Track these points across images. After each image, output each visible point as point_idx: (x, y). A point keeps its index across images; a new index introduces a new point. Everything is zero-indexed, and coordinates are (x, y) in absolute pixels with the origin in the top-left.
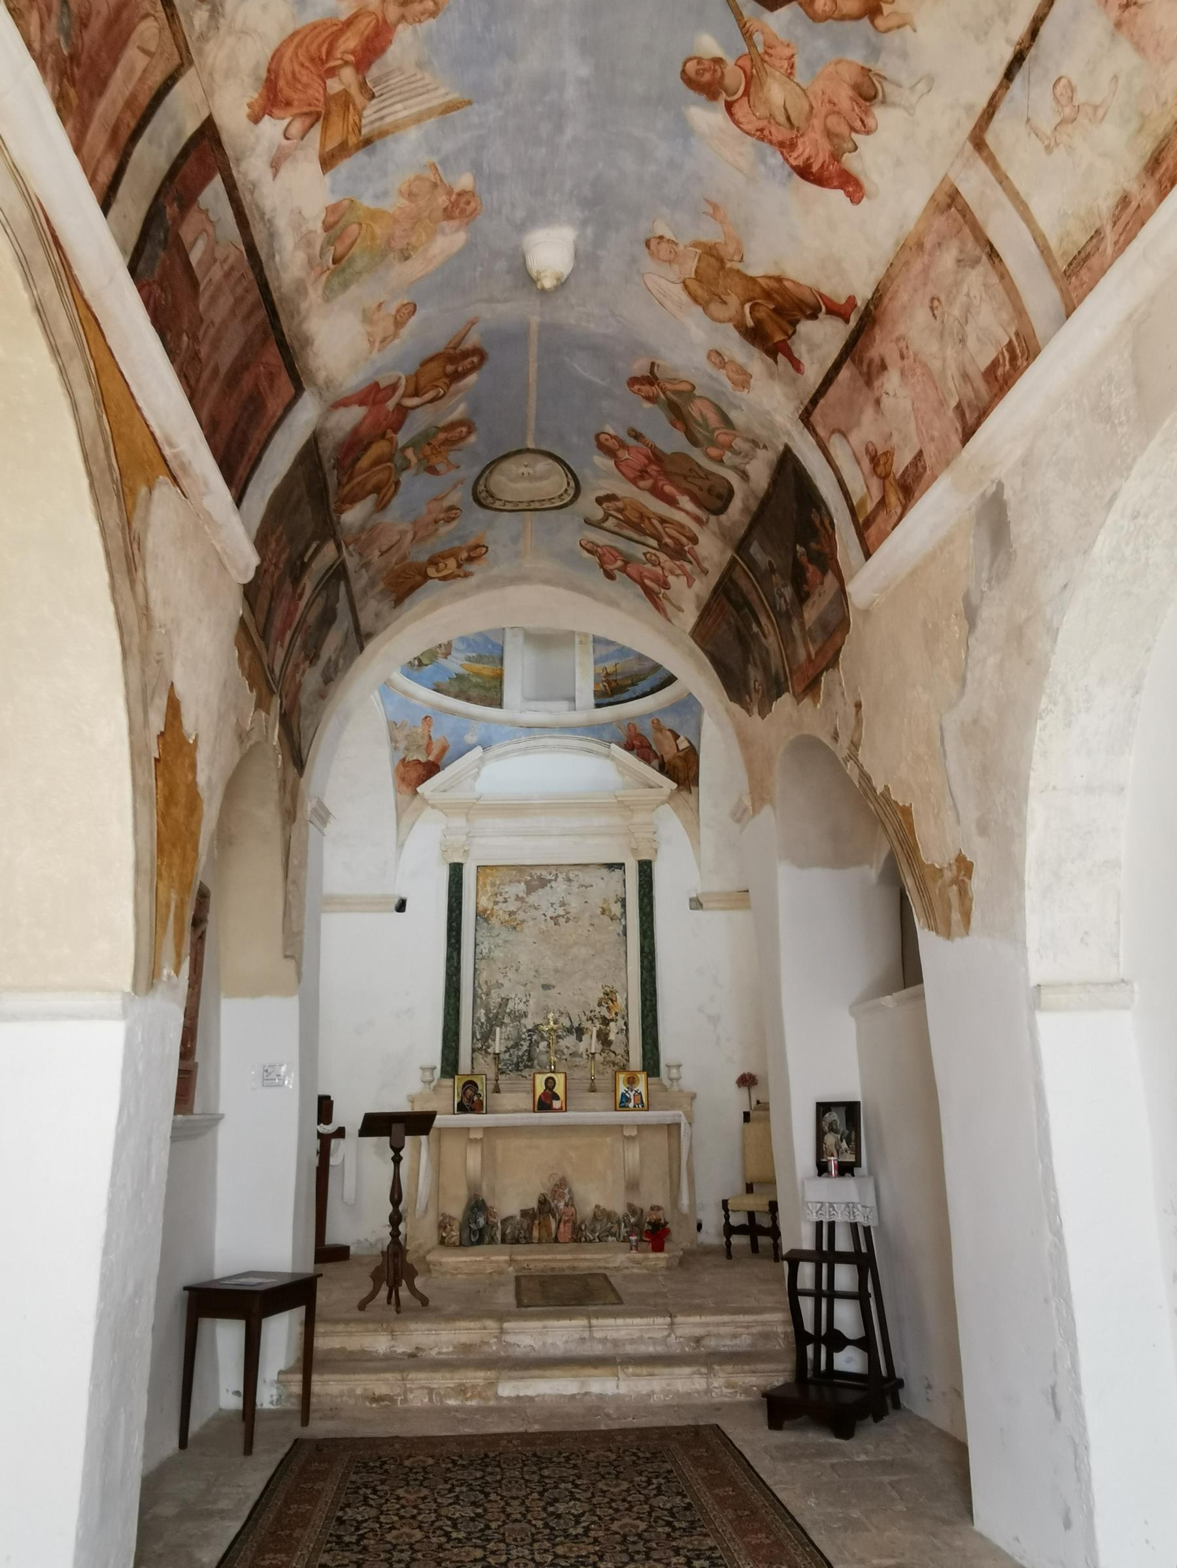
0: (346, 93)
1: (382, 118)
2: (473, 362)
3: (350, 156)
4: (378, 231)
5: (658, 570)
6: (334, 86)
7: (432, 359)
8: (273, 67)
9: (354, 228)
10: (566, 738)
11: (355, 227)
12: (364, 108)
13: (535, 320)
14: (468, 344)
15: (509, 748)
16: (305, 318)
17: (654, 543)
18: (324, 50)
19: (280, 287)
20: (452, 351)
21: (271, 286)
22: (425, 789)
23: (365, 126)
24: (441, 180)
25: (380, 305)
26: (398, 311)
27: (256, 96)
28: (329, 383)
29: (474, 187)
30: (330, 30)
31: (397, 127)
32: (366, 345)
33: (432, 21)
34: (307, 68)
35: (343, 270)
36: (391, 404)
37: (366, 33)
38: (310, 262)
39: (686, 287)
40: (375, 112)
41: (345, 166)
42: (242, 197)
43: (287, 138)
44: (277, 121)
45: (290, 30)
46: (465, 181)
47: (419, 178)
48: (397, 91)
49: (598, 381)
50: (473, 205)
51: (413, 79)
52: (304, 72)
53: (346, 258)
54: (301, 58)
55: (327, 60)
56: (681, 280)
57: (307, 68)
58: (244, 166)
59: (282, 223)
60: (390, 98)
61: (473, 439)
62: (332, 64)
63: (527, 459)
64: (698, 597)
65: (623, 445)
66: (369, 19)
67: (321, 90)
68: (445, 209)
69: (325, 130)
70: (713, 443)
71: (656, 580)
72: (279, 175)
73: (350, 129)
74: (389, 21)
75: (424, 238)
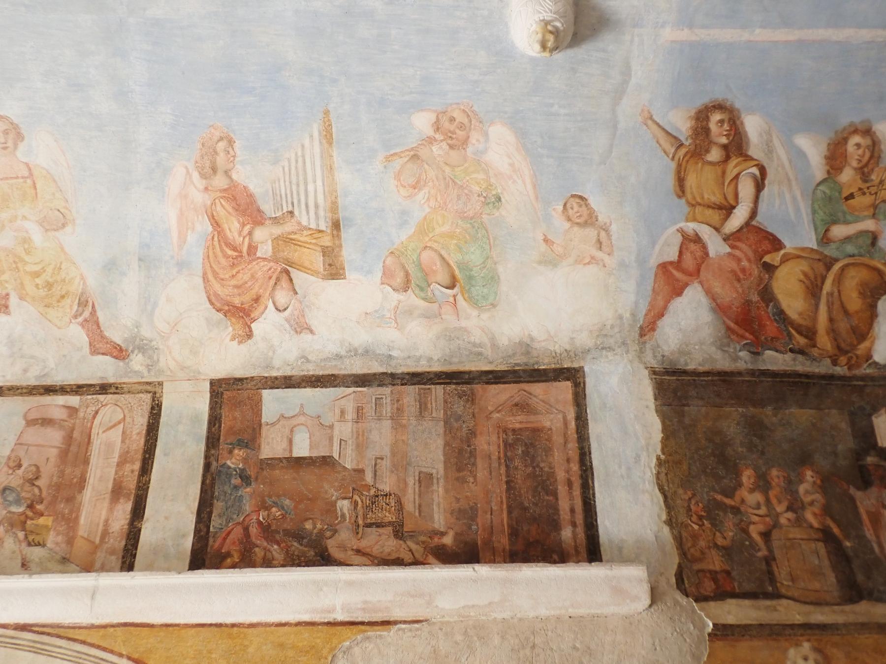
0: (276, 240)
1: (317, 206)
2: (721, 122)
3: (340, 246)
4: (446, 228)
6: (265, 250)
7: (681, 181)
8: (218, 305)
9: (426, 255)
11: (426, 255)
12: (299, 223)
13: (668, 34)
16: (493, 340)
18: (230, 252)
19: (430, 359)
20: (683, 151)
21: (419, 369)
23: (318, 225)
24: (412, 149)
25: (546, 240)
26: (569, 219)
27: (231, 329)
28: (601, 332)
29: (435, 111)
30: (216, 243)
31: (332, 193)
32: (593, 269)
33: (237, 145)
34: (238, 272)
36: (716, 247)
37: (231, 210)
38: (427, 316)
40: (308, 212)
41: (349, 253)
42: (302, 373)
43: (285, 309)
44: (264, 316)
45: (200, 281)
46: (423, 122)
47: (398, 176)
48: (294, 187)
50: (456, 114)
51: (287, 169)
52: (240, 275)
53: (457, 272)
54: (227, 276)
55: (241, 252)
57: (238, 272)
58: (277, 363)
59: (361, 338)
60: (298, 194)
62: (245, 249)
66: (219, 208)
67: (262, 264)
68: (451, 147)
69: (301, 268)
72: (313, 328)
73: (314, 241)
74: (226, 187)
75: (481, 176)
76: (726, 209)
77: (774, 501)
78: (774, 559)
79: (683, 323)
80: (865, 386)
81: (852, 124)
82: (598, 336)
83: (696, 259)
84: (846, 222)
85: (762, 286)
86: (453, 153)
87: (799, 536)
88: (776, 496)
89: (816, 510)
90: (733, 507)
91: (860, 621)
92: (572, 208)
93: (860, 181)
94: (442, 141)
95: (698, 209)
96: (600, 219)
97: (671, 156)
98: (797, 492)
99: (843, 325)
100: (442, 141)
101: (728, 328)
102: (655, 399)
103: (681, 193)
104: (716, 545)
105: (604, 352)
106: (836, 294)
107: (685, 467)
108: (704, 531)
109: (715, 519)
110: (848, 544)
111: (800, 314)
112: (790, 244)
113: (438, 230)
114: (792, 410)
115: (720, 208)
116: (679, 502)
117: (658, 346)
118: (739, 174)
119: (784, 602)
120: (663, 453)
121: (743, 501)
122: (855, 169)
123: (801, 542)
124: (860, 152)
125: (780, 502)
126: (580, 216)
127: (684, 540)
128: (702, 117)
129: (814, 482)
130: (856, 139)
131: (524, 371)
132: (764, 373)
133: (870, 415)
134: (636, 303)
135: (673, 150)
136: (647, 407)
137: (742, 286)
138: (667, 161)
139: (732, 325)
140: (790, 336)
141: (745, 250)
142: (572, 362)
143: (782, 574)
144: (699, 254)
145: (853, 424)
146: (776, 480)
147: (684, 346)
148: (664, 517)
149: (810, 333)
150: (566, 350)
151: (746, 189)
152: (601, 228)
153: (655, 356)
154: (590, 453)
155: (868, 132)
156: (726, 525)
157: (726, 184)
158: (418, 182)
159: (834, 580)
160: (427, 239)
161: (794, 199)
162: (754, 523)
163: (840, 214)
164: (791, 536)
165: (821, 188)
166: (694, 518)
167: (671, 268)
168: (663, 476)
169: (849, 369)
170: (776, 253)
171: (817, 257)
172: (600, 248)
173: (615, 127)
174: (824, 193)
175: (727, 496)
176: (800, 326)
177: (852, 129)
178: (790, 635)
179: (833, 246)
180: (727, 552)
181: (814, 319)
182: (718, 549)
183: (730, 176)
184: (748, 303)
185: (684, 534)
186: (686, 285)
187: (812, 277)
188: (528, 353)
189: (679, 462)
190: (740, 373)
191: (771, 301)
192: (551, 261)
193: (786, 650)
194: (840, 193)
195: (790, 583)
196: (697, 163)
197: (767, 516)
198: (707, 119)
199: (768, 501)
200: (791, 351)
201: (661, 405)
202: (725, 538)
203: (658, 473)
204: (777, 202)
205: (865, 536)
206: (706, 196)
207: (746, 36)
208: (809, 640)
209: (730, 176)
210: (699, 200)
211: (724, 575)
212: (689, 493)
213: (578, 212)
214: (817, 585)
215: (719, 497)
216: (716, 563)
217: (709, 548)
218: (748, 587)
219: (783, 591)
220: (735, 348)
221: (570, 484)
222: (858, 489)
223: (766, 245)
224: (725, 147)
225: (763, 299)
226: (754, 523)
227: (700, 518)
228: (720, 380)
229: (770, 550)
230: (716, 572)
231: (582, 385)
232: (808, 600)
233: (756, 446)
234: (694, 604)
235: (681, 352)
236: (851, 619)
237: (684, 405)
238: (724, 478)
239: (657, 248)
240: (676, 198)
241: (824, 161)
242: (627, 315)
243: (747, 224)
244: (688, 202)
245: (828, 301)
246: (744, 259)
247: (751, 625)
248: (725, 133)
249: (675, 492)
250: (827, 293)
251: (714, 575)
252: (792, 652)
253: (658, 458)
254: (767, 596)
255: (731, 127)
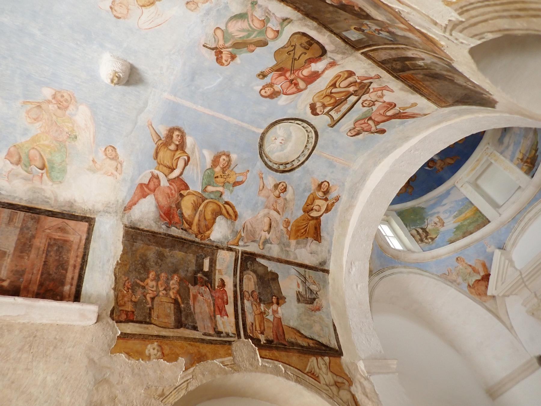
2: (178, 135)
4: (46, 143)
5: (378, 104)
7: (157, 153)
9: (32, 152)
10: (536, 206)
13: (166, 95)
14: (163, 132)
15: (514, 237)
17: (353, 98)
19: (21, 199)
20: (160, 142)
21: (14, 202)
22: (491, 291)
24: (38, 103)
25: (93, 161)
26: (106, 155)
28: (108, 205)
29: (55, 90)
35: (52, 167)
36: (164, 182)
38: (25, 179)
39: (143, 6)
46: (47, 93)
47: (28, 112)
49: (219, 80)
50: (65, 94)
53: (47, 164)
56: (140, 7)
61: (234, 157)
63: (270, 136)
64: (401, 89)
65: (271, 85)
68: (59, 108)
70: (263, 30)
71: (388, 109)
75: (70, 125)
76: (171, 169)
77: (160, 286)
78: (153, 309)
79: (143, 209)
80: (205, 247)
81: (224, 151)
82: (105, 206)
83: (155, 185)
84: (213, 186)
85: (178, 202)
86: (59, 111)
87: (165, 301)
88: (161, 284)
89: (175, 291)
90: (143, 286)
91: (179, 336)
92: (109, 151)
93: (221, 173)
94: (55, 104)
95: (161, 166)
96: (119, 158)
97: (155, 142)
98: (169, 284)
99: (203, 223)
100: (55, 104)
101: (161, 215)
102: (123, 238)
103: (156, 158)
104: (131, 301)
105: (107, 214)
106: (203, 211)
107: (128, 267)
108: (128, 294)
109: (134, 290)
110: (183, 306)
111: (189, 216)
112: (192, 189)
113: (42, 142)
114: (176, 252)
115: (169, 168)
116: (121, 281)
117: (130, 216)
118: (180, 157)
119: (152, 326)
120: (120, 260)
121: (147, 284)
122: (221, 168)
123: (165, 303)
124: (224, 162)
125: (162, 286)
126: (111, 155)
127: (119, 296)
128: (171, 131)
129: (177, 281)
130: (224, 157)
131: (67, 214)
132: (169, 235)
133: (204, 258)
134: (126, 197)
135: (157, 140)
136: (119, 240)
137: (170, 200)
138: (154, 144)
139: (162, 214)
140: (183, 223)
141: (175, 187)
142: (91, 215)
143: (154, 315)
144: (157, 183)
145: (197, 260)
146: (163, 278)
147: (141, 218)
148: (113, 286)
149: (190, 224)
150: (90, 209)
151: (181, 164)
152: (119, 163)
153: (128, 220)
154: (88, 255)
155: (228, 156)
156: (138, 293)
157: (174, 160)
158: (37, 118)
159: (174, 319)
160: (35, 144)
161: (197, 172)
162: (149, 293)
163: (212, 183)
164: (162, 300)
165: (207, 171)
166: (126, 288)
167: (144, 186)
168: (117, 270)
169: (201, 240)
170: (186, 191)
171: (200, 196)
172: (117, 171)
173: (136, 123)
174: (208, 173)
175: (142, 281)
176: (188, 220)
177: (223, 153)
178: (150, 339)
179: (207, 193)
180: (135, 303)
181: (193, 219)
182: (132, 302)
183: (176, 157)
184: (171, 207)
185: (119, 295)
186: (148, 194)
187: (196, 203)
188: (71, 207)
189: (126, 265)
190: (160, 234)
191: (179, 209)
192: (93, 170)
193: (147, 345)
194: (214, 175)
195: (157, 319)
196: (165, 148)
197: (155, 291)
198: (173, 133)
199: (157, 285)
200: (182, 229)
201: (125, 240)
202: (136, 298)
203: (116, 268)
204: (191, 172)
205: (189, 303)
206: (165, 162)
207: (194, 107)
208: (157, 342)
209: (176, 157)
210: (162, 163)
211: (131, 313)
212: (127, 278)
213: (111, 153)
214: (166, 321)
215: (138, 281)
216: (129, 307)
217: (128, 301)
218: (140, 319)
219: (153, 322)
220: (161, 223)
221: (75, 267)
222: (192, 285)
223: (183, 187)
224: (177, 145)
225: (176, 207)
226: (149, 293)
227: (128, 288)
228: (152, 235)
229: (153, 305)
230: (128, 311)
231: (93, 225)
232: (161, 326)
233: (158, 263)
234: (115, 324)
235: (139, 221)
236: (176, 334)
237: (135, 242)
238: (142, 274)
239: (140, 177)
240: (153, 159)
241: (211, 162)
242: (121, 201)
243: (178, 177)
244: (158, 163)
245: (200, 213)
246: (173, 190)
247: (136, 334)
248: (178, 140)
249: (121, 277)
250: (200, 210)
251: (127, 313)
252: (149, 346)
253: (117, 262)
254: (146, 323)
255: (181, 138)
